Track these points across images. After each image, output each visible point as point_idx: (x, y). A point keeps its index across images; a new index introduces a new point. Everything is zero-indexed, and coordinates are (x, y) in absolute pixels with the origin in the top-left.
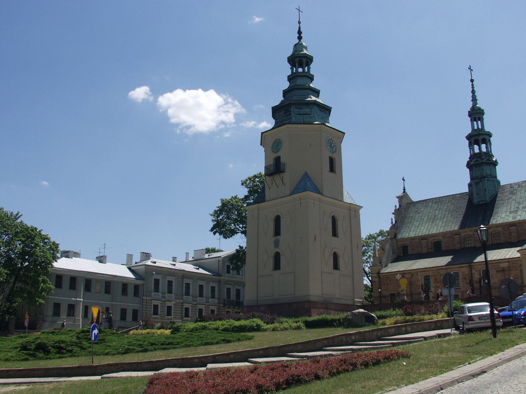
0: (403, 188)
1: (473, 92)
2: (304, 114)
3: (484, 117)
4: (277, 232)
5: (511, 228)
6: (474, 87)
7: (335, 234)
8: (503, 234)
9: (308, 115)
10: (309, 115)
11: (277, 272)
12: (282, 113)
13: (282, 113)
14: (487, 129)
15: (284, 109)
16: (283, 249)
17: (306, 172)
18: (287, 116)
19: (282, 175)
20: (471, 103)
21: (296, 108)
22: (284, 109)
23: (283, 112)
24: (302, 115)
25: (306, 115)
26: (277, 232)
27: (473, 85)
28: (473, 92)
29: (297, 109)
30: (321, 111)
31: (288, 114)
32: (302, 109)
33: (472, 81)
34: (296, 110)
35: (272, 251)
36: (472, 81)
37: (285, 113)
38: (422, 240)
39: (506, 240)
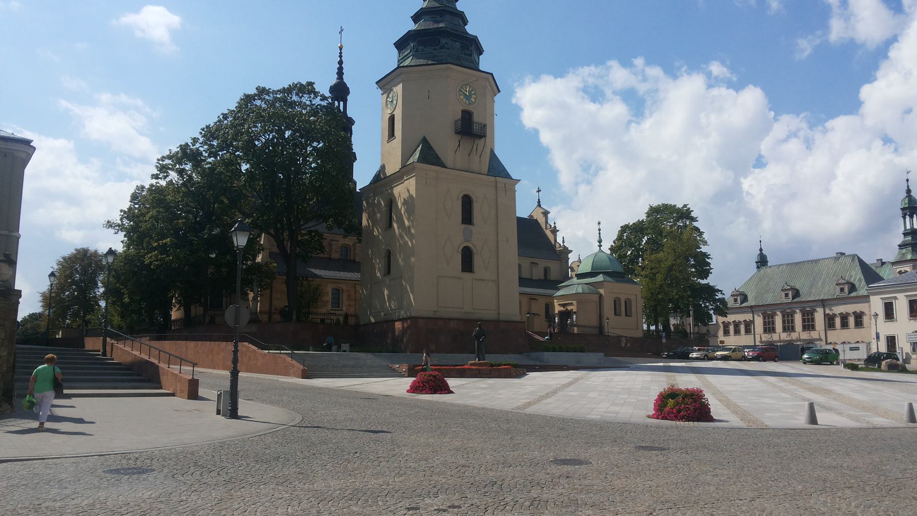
0: (537, 201)
1: (341, 63)
3: (349, 98)
4: (467, 218)
6: (342, 56)
11: (467, 276)
13: (457, 45)
14: (350, 114)
16: (476, 244)
18: (465, 54)
20: (336, 76)
23: (458, 43)
26: (467, 218)
27: (341, 53)
28: (341, 63)
31: (467, 52)
33: (341, 48)
35: (459, 242)
36: (341, 48)
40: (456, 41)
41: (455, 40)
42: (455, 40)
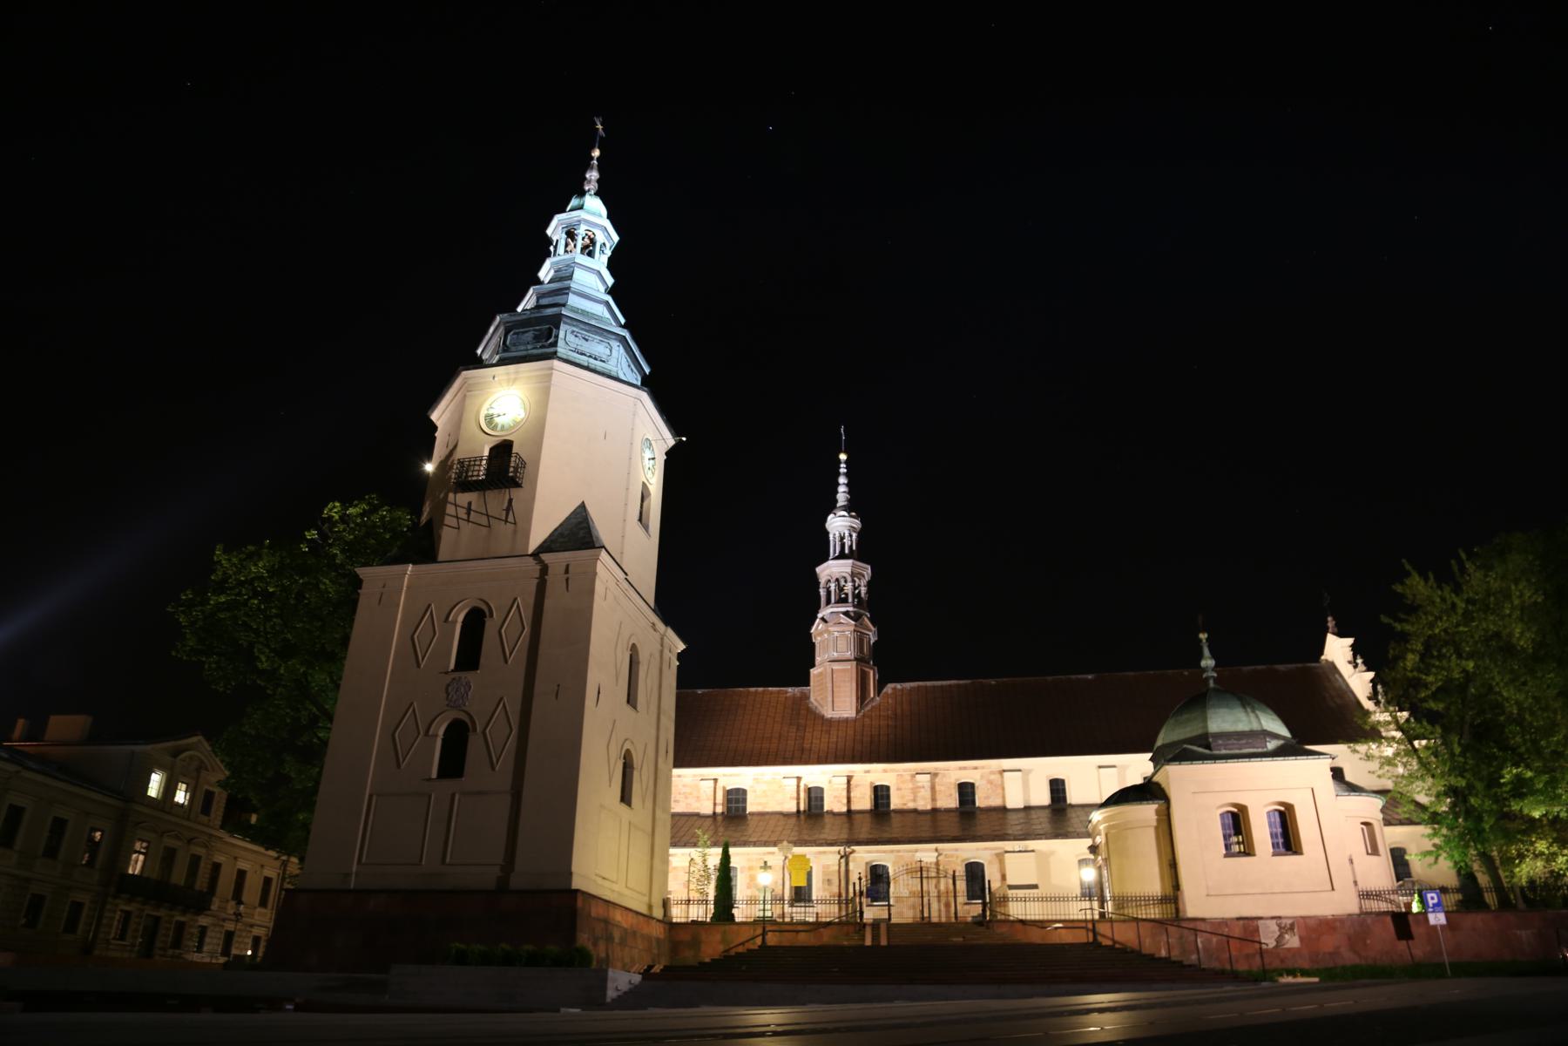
2: (590, 356)
5: (919, 777)
7: (631, 700)
8: (899, 789)
9: (601, 361)
10: (604, 361)
12: (529, 336)
13: (529, 336)
15: (537, 328)
17: (583, 502)
19: (515, 493)
21: (573, 332)
22: (537, 328)
24: (585, 355)
25: (595, 359)
29: (576, 336)
30: (629, 366)
32: (587, 340)
34: (570, 338)
37: (537, 338)
38: (702, 780)
39: (905, 804)
40: (526, 332)
41: (522, 330)
42: (522, 330)
